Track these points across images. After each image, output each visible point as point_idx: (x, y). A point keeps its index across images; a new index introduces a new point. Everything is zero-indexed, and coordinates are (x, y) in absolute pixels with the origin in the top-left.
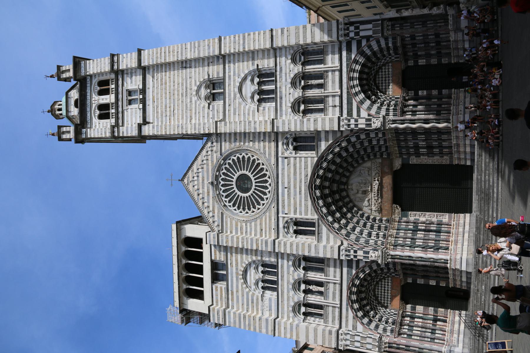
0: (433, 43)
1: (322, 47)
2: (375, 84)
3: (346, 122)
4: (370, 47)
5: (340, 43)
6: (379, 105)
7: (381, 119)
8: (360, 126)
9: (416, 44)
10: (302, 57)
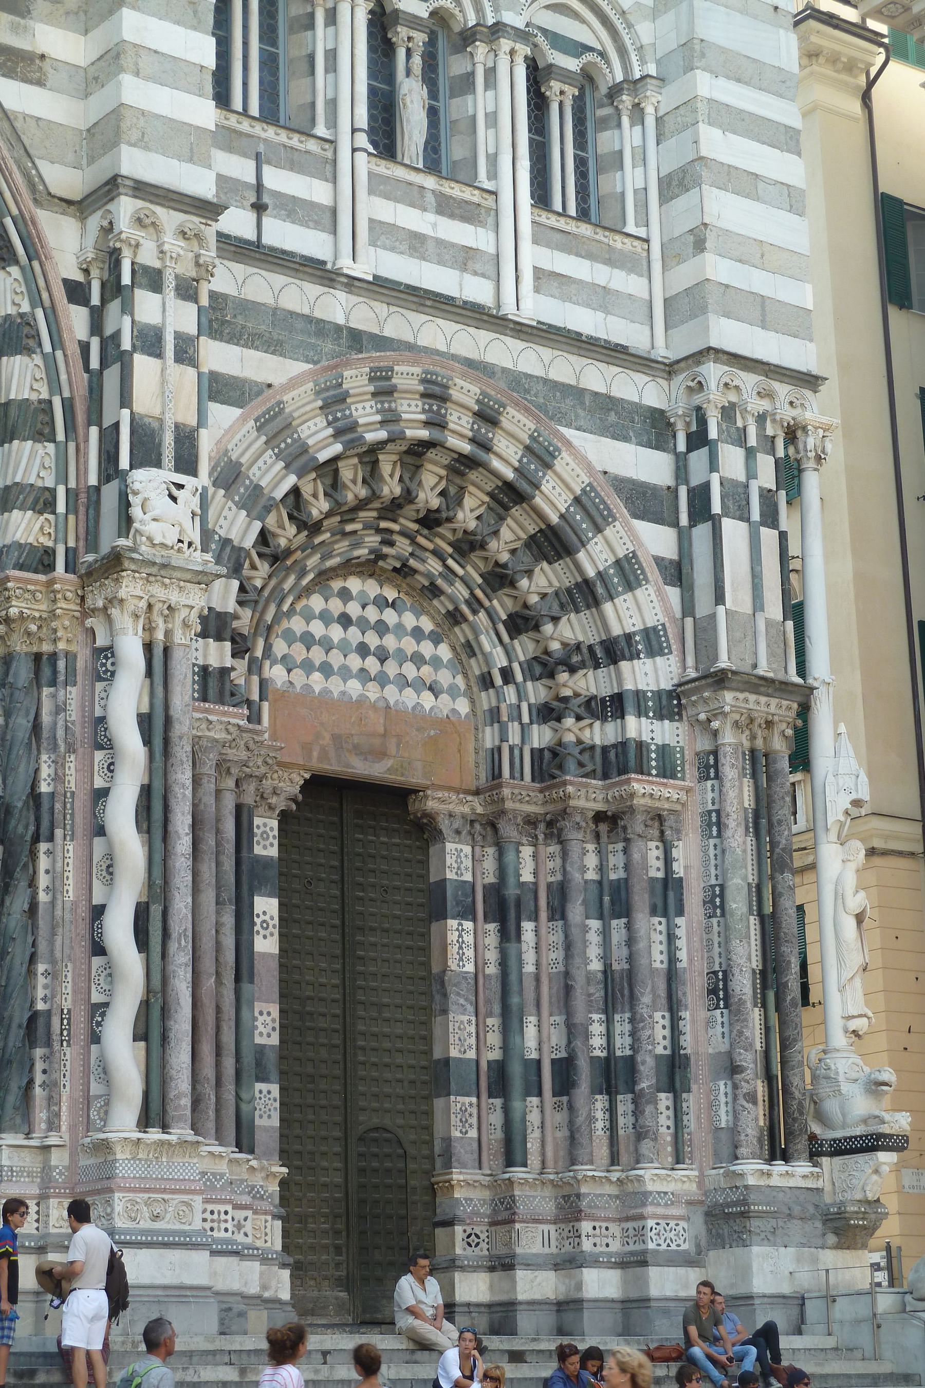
0: (609, 1036)
1: (631, 228)
2: (349, 567)
3: (187, 269)
4: (628, 572)
5: (670, 369)
10: (572, 64)
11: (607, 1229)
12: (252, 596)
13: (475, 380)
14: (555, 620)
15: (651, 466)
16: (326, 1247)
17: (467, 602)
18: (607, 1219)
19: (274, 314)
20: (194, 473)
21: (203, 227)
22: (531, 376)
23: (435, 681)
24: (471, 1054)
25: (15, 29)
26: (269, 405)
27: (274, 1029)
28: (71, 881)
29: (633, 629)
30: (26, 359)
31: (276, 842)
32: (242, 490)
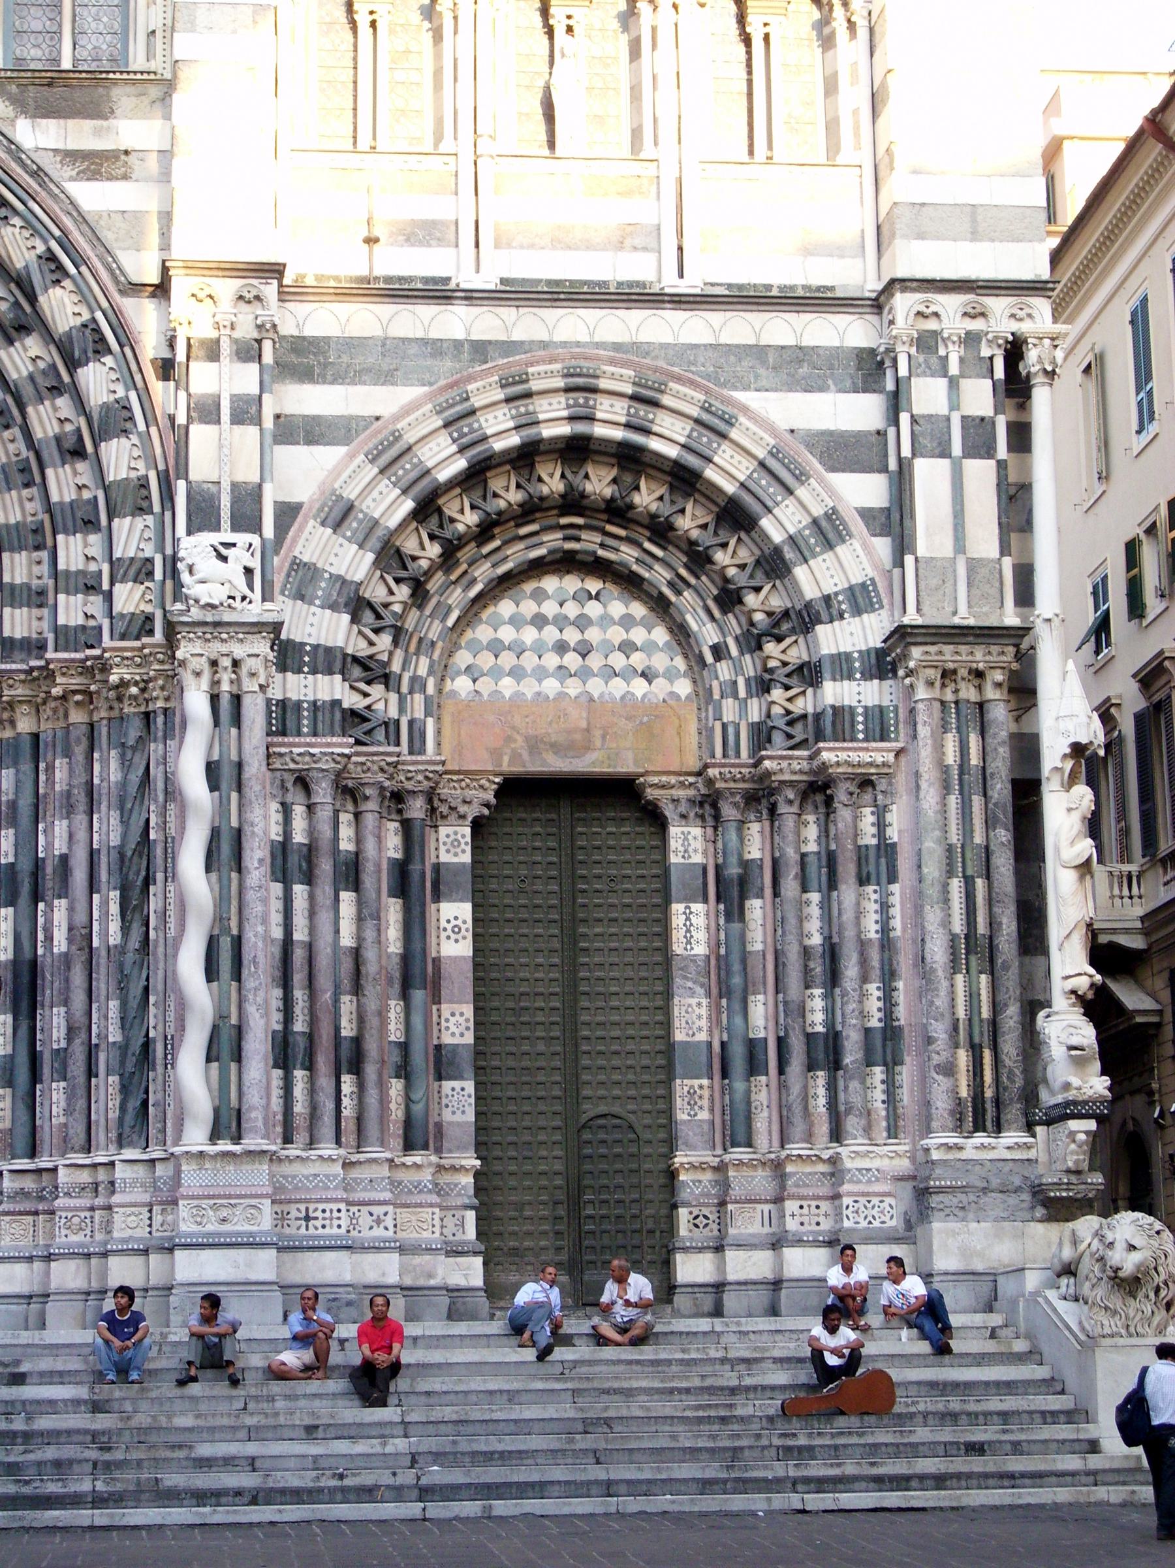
0: (830, 1011)
2: (537, 568)
3: (246, 331)
4: (828, 531)
6: (377, 593)
7: (256, 610)
8: (201, 437)
9: (832, 883)
11: (818, 1207)
12: (389, 620)
13: (625, 364)
14: (758, 590)
15: (860, 412)
16: (545, 1233)
17: (671, 584)
18: (818, 1198)
19: (383, 345)
20: (257, 528)
21: (262, 287)
22: (696, 346)
23: (649, 667)
24: (702, 1037)
25: (97, 132)
26: (380, 437)
27: (468, 1029)
28: (172, 919)
29: (835, 589)
30: (123, 440)
31: (468, 849)
32: (355, 525)
